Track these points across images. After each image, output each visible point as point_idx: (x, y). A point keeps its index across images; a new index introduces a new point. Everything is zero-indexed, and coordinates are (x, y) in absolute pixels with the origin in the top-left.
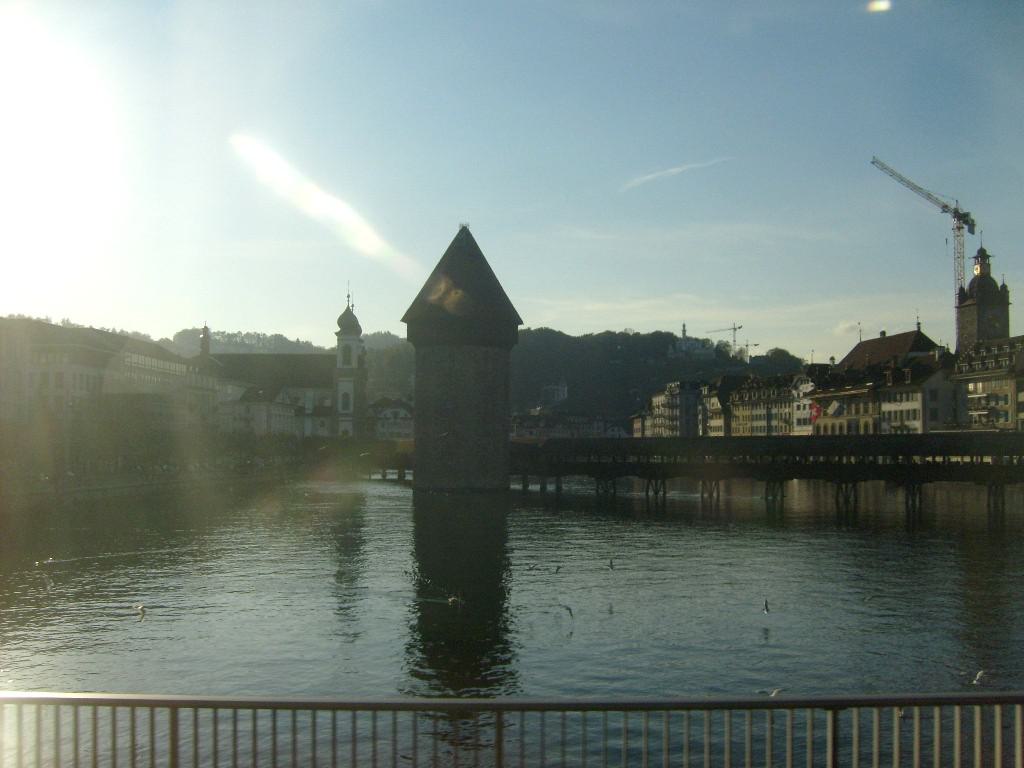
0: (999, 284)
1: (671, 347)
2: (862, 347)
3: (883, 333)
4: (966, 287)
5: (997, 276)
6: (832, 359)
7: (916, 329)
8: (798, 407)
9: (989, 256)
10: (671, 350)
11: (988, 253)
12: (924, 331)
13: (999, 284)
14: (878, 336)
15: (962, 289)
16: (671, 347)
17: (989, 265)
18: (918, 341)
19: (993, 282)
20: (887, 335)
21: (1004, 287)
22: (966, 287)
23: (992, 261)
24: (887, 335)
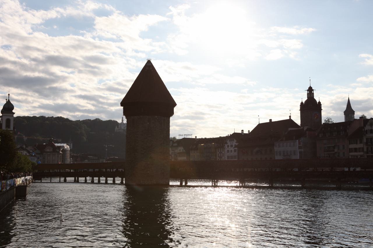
0: (318, 101)
1: (116, 127)
2: (261, 127)
3: (271, 120)
4: (304, 102)
5: (317, 97)
6: (249, 131)
7: (288, 118)
8: (228, 151)
9: (313, 90)
10: (116, 128)
11: (313, 89)
12: (291, 118)
13: (318, 101)
14: (268, 121)
15: (302, 103)
16: (116, 127)
17: (313, 93)
18: (290, 122)
19: (315, 100)
20: (273, 121)
21: (319, 102)
22: (304, 102)
23: (315, 92)
24: (273, 121)
